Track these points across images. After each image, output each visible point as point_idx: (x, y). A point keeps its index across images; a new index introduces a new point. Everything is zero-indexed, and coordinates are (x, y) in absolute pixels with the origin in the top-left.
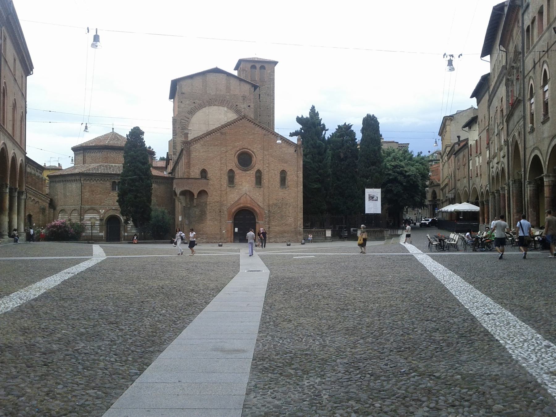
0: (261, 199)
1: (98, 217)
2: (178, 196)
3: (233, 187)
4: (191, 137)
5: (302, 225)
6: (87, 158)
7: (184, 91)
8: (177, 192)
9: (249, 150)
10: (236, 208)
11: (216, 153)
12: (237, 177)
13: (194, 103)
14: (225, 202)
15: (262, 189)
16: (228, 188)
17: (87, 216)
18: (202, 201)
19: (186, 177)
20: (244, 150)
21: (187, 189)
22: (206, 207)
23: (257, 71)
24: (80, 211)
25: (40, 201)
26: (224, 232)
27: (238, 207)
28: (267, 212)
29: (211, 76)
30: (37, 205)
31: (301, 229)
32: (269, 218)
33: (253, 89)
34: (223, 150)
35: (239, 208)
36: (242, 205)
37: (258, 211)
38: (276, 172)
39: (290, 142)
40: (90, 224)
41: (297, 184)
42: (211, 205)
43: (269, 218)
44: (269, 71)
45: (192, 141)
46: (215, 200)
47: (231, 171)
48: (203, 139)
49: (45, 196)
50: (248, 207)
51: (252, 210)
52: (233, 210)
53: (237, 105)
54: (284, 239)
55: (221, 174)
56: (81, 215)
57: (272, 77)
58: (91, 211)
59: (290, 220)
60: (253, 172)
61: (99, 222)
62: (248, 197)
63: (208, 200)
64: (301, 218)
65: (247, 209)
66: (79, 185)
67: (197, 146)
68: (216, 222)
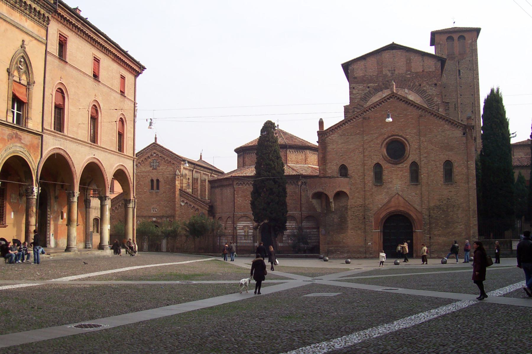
3: (381, 186)
4: (326, 128)
5: (477, 234)
6: (246, 159)
9: (401, 136)
10: (384, 213)
11: (357, 143)
12: (385, 172)
13: (368, 87)
14: (371, 206)
15: (419, 187)
16: (374, 186)
17: (240, 225)
18: (341, 205)
19: (322, 175)
20: (393, 137)
21: (320, 190)
22: (347, 212)
23: (456, 43)
24: (233, 218)
25: (199, 208)
26: (370, 244)
27: (388, 211)
28: (426, 217)
29: (386, 55)
30: (197, 212)
32: (430, 224)
33: (439, 64)
34: (366, 140)
35: (390, 213)
36: (393, 209)
37: (414, 217)
39: (456, 123)
40: (243, 233)
41: (468, 178)
42: (353, 210)
44: (470, 41)
45: (329, 130)
47: (378, 166)
49: (204, 203)
50: (400, 211)
52: (381, 216)
53: (420, 85)
55: (364, 170)
56: (234, 223)
57: (474, 48)
58: (244, 218)
59: (459, 227)
60: (406, 165)
61: (252, 231)
62: (400, 198)
63: (349, 204)
64: (475, 225)
65: (400, 213)
66: (232, 190)
67: (335, 136)
68: (359, 232)
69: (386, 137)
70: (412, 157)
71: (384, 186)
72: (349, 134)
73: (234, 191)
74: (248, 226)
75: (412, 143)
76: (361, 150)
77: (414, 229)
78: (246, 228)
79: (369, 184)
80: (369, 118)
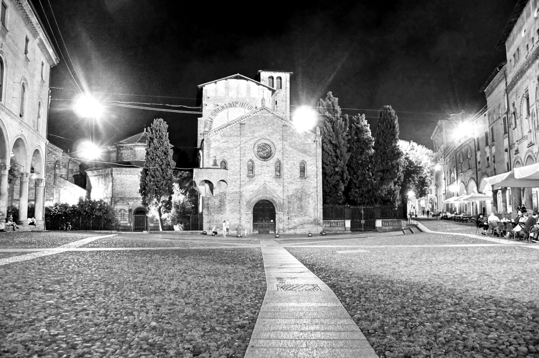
0: (281, 188)
1: (127, 208)
2: (198, 186)
7: (208, 96)
8: (196, 182)
10: (254, 199)
18: (221, 191)
22: (226, 198)
27: (257, 197)
31: (321, 221)
32: (289, 208)
34: (242, 141)
37: (277, 202)
38: (295, 162)
43: (289, 208)
46: (235, 190)
47: (251, 160)
48: (223, 129)
51: (272, 201)
52: (252, 201)
54: (303, 230)
69: (257, 139)
70: (277, 156)
71: (255, 178)
72: (229, 136)
73: (113, 179)
74: (124, 210)
75: (277, 146)
76: (238, 148)
77: (276, 211)
78: (123, 210)
79: (244, 175)
80: (245, 124)
